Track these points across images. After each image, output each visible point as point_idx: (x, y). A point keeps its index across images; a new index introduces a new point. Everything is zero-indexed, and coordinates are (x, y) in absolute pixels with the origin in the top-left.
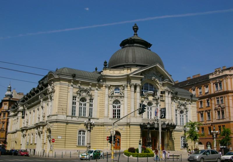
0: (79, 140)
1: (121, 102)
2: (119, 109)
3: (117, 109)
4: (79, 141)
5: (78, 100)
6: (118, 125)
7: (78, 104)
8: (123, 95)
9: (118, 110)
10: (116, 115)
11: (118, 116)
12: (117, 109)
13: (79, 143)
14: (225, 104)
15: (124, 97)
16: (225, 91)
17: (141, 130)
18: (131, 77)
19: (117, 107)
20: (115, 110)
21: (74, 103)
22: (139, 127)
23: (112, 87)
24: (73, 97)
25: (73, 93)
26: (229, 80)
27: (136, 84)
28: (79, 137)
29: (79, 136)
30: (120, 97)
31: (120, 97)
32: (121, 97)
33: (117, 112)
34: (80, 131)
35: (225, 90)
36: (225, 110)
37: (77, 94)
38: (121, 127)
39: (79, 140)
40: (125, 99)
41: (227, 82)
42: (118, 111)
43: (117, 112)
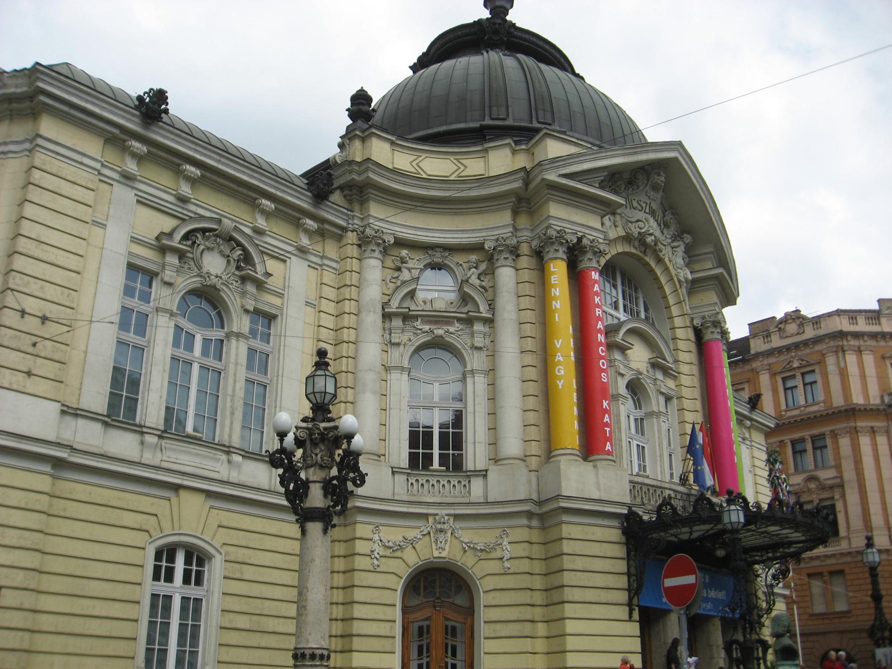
0: (158, 630)
4: (150, 640)
5: (165, 297)
6: (457, 517)
7: (162, 331)
8: (483, 307)
10: (436, 451)
11: (443, 459)
13: (149, 651)
14: (838, 467)
16: (835, 405)
17: (629, 558)
18: (554, 187)
21: (133, 321)
22: (615, 534)
24: (132, 268)
25: (134, 240)
26: (851, 359)
27: (580, 240)
28: (153, 606)
29: (155, 596)
30: (459, 320)
31: (459, 320)
32: (469, 321)
34: (166, 553)
35: (838, 401)
36: (843, 496)
37: (163, 250)
38: (469, 534)
39: (152, 624)
41: (842, 365)
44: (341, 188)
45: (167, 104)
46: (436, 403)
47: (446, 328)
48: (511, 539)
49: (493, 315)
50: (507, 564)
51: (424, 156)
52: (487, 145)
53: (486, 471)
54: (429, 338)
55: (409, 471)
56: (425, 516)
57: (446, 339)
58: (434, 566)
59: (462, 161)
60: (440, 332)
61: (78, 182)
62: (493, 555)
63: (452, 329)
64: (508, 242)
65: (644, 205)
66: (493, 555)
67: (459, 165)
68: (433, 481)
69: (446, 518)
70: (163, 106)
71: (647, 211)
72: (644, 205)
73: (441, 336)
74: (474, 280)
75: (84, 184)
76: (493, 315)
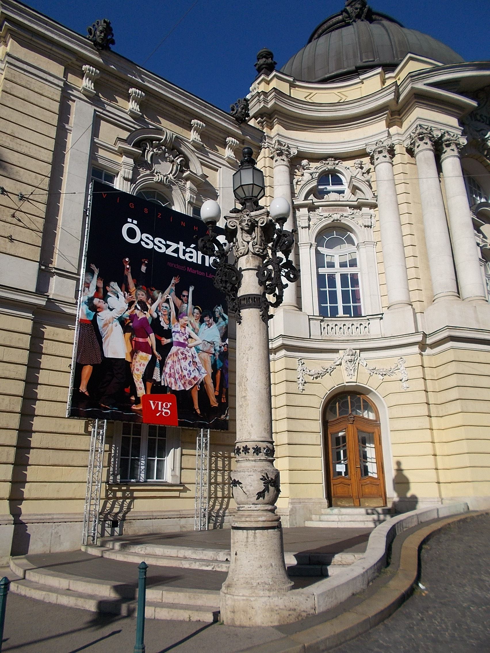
1: (360, 235)
2: (349, 270)
3: (338, 271)
6: (362, 350)
9: (344, 277)
11: (346, 310)
12: (338, 271)
15: (374, 206)
19: (337, 265)
20: (332, 278)
23: (305, 162)
31: (350, 207)
33: (339, 289)
40: (385, 215)
42: (344, 284)
43: (339, 289)
44: (255, 117)
45: (113, 36)
46: (337, 269)
47: (341, 213)
48: (406, 365)
49: (377, 201)
50: (405, 384)
51: (314, 92)
52: (362, 77)
53: (382, 314)
54: (330, 222)
55: (322, 318)
56: (336, 351)
57: (342, 221)
58: (346, 390)
59: (343, 93)
60: (336, 217)
61: (45, 94)
62: (393, 378)
63: (345, 214)
64: (385, 144)
65: (485, 119)
66: (393, 378)
67: (342, 96)
68: (340, 324)
69: (354, 351)
70: (109, 37)
71: (488, 123)
72: (485, 119)
73: (337, 220)
74: (359, 176)
75: (50, 96)
76: (377, 201)
